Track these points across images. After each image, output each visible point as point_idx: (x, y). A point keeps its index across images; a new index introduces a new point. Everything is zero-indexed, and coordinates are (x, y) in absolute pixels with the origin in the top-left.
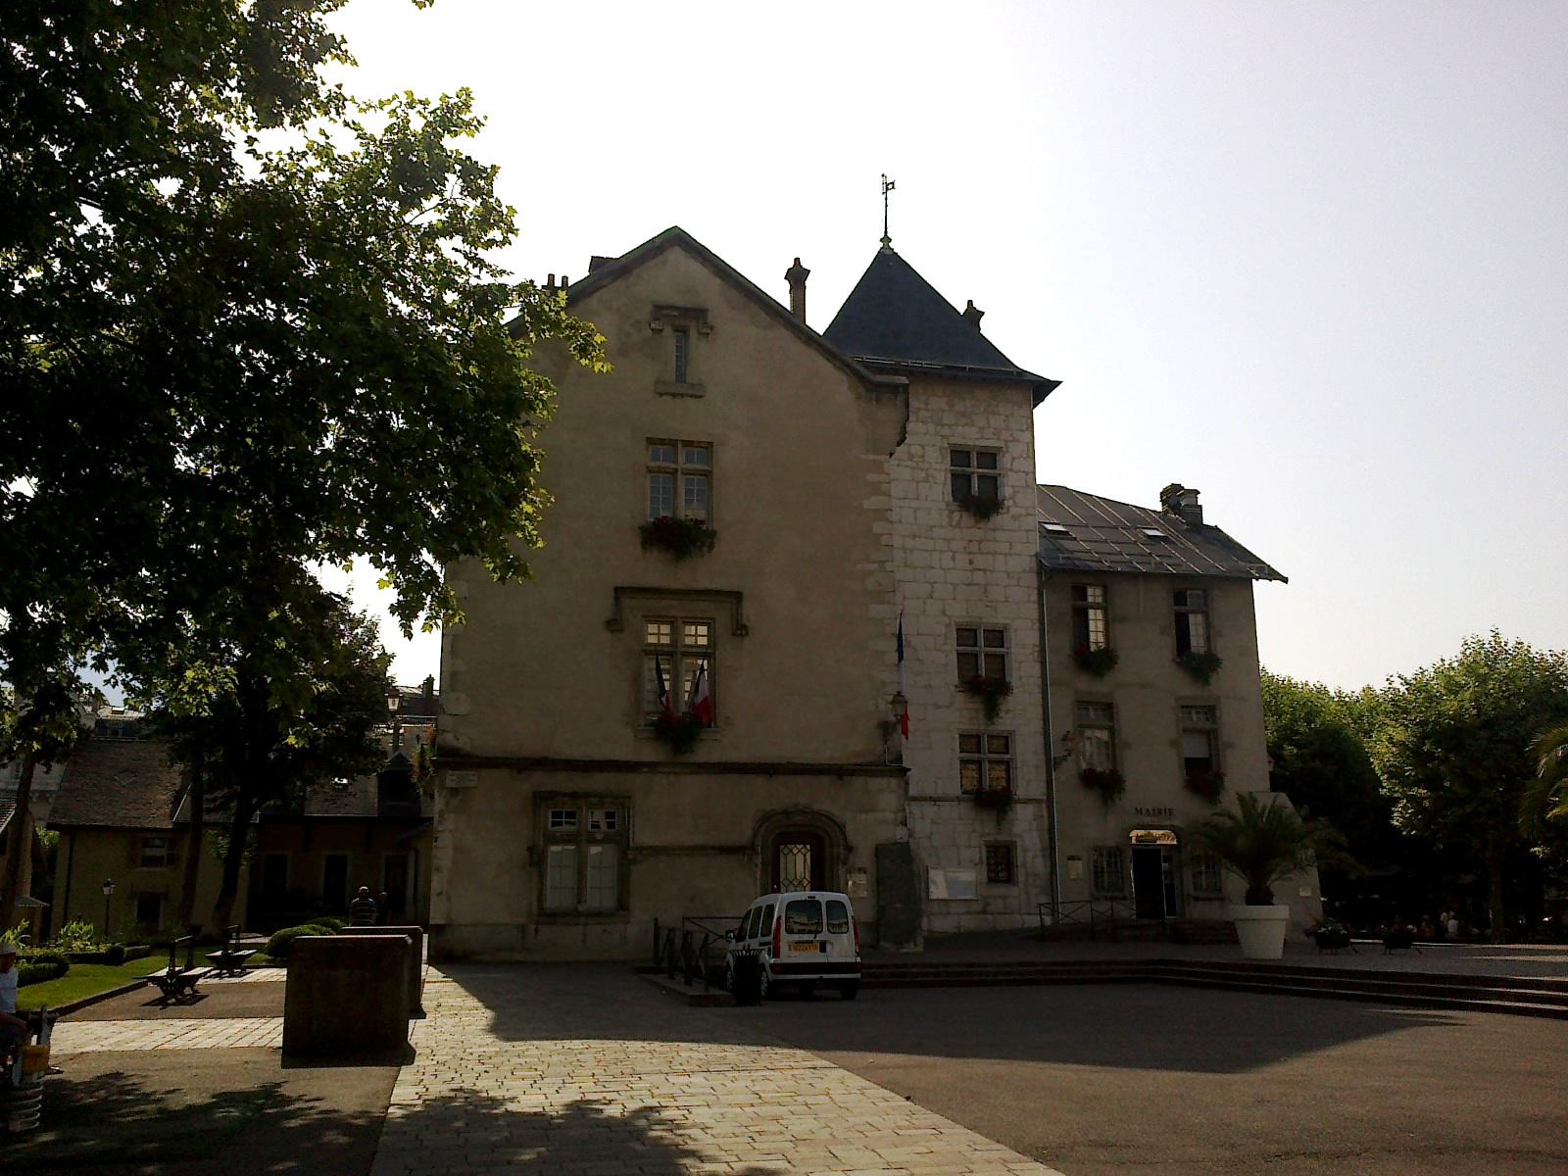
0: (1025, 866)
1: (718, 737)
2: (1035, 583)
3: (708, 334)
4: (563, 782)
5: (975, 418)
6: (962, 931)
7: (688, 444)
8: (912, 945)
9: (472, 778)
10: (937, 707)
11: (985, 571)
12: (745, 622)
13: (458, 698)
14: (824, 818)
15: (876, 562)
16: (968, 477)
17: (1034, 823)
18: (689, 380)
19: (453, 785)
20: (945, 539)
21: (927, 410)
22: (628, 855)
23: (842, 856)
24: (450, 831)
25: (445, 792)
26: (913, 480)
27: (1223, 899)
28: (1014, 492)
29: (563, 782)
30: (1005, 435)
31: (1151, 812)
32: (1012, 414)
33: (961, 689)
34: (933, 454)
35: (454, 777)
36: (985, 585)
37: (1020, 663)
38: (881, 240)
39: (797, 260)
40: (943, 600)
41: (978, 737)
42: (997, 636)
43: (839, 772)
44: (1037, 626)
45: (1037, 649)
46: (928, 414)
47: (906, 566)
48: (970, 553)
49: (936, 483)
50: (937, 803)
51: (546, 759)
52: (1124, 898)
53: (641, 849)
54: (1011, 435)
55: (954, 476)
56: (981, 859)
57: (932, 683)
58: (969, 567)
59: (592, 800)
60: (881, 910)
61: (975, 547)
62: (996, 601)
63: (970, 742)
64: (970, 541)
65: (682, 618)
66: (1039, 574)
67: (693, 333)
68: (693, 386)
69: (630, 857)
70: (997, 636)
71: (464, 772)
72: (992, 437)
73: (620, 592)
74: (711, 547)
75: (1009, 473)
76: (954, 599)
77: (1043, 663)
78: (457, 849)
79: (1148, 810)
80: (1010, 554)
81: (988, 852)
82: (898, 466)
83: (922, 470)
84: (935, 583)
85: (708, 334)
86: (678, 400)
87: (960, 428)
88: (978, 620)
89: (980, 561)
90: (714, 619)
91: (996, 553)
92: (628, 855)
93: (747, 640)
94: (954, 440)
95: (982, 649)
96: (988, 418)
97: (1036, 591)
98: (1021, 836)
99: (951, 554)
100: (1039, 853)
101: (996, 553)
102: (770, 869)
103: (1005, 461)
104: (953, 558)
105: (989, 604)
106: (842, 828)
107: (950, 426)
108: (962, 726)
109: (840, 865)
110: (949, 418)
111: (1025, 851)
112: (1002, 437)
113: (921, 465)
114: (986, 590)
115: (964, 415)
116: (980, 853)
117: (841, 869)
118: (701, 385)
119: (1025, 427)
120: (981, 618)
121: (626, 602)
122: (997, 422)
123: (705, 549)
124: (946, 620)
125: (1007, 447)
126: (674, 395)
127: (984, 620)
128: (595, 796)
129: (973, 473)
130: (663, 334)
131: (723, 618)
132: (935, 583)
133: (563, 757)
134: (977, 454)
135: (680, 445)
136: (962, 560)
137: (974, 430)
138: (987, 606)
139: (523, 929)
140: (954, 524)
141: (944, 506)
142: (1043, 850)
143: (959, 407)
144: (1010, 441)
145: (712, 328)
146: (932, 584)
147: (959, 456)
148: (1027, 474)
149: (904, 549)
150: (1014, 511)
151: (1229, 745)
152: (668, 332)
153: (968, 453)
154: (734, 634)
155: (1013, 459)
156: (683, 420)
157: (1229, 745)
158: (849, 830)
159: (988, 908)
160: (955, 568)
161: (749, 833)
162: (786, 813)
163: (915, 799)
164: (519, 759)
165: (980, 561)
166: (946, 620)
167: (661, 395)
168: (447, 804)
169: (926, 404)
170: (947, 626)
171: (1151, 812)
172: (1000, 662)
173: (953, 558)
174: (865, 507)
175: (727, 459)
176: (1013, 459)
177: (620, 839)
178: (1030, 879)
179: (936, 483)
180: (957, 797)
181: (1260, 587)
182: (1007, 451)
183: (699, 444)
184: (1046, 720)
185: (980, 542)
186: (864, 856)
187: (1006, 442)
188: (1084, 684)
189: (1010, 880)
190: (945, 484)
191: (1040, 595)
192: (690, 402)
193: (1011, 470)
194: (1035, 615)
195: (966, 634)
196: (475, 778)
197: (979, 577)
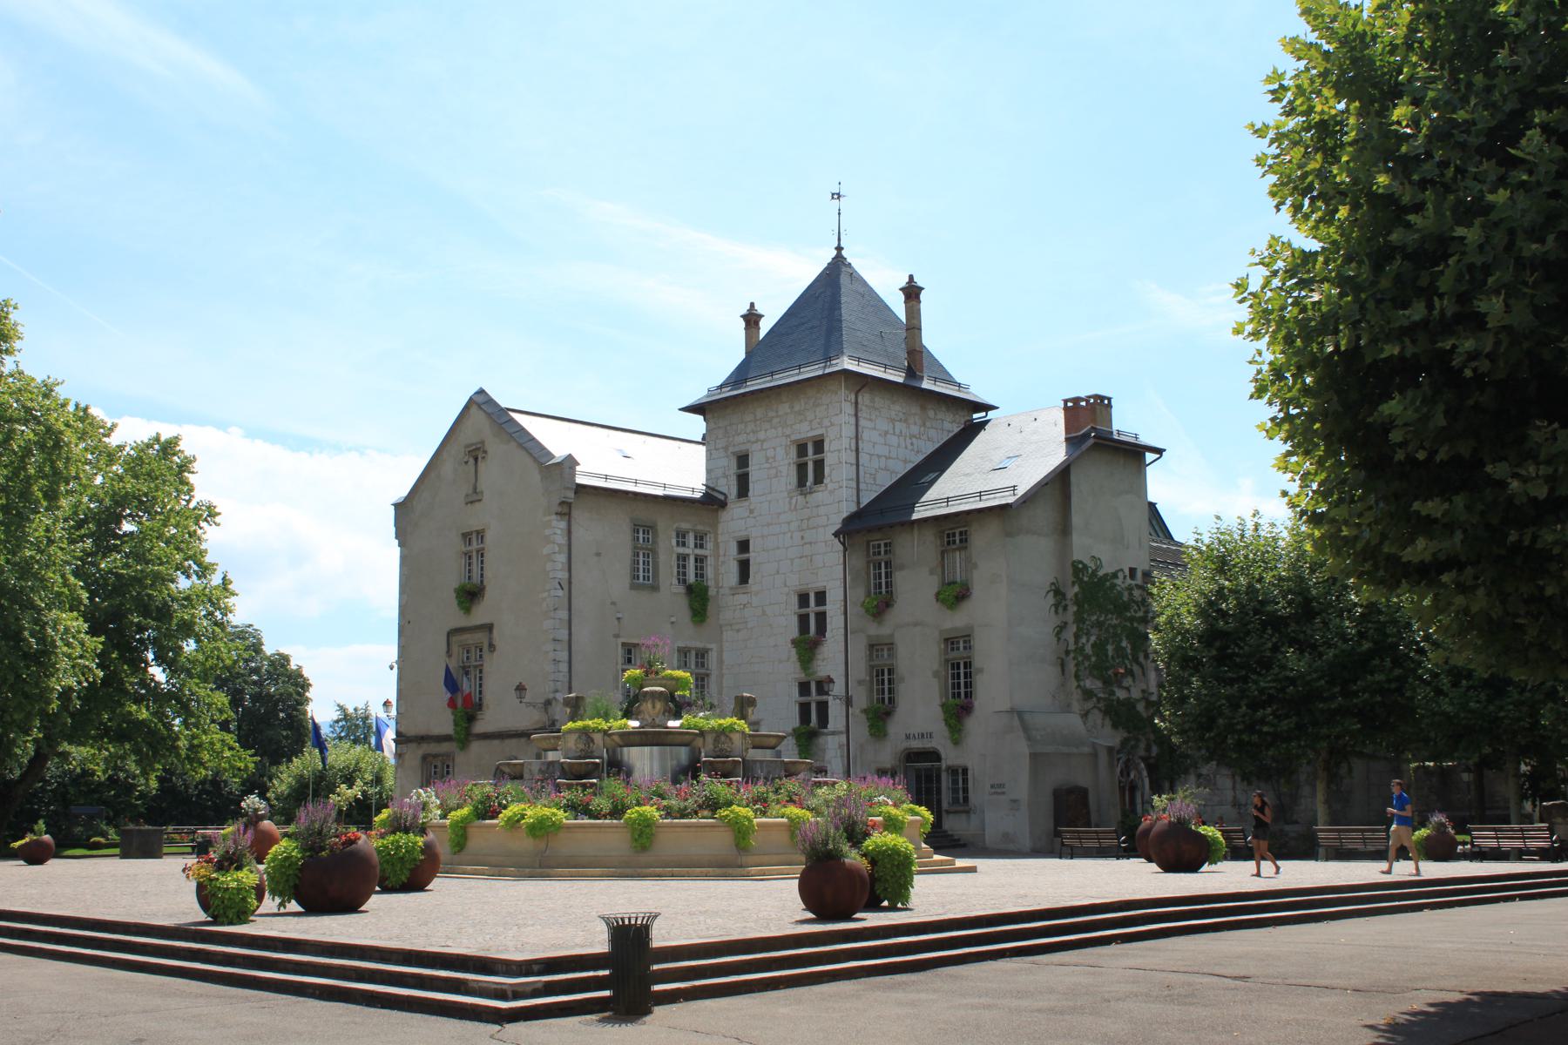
10: (780, 661)
11: (811, 543)
21: (777, 416)
27: (967, 812)
30: (826, 422)
34: (781, 452)
63: (804, 688)
70: (821, 597)
93: (495, 654)
95: (813, 607)
98: (830, 763)
99: (789, 534)
104: (791, 537)
108: (797, 676)
113: (774, 465)
124: (786, 589)
126: (472, 502)
127: (810, 586)
137: (807, 423)
140: (793, 507)
141: (786, 494)
149: (763, 536)
150: (830, 486)
151: (981, 671)
155: (831, 441)
156: (474, 519)
157: (981, 671)
166: (786, 589)
167: (467, 504)
170: (787, 594)
173: (791, 537)
176: (831, 441)
185: (808, 519)
187: (826, 427)
192: (477, 504)
195: (803, 599)
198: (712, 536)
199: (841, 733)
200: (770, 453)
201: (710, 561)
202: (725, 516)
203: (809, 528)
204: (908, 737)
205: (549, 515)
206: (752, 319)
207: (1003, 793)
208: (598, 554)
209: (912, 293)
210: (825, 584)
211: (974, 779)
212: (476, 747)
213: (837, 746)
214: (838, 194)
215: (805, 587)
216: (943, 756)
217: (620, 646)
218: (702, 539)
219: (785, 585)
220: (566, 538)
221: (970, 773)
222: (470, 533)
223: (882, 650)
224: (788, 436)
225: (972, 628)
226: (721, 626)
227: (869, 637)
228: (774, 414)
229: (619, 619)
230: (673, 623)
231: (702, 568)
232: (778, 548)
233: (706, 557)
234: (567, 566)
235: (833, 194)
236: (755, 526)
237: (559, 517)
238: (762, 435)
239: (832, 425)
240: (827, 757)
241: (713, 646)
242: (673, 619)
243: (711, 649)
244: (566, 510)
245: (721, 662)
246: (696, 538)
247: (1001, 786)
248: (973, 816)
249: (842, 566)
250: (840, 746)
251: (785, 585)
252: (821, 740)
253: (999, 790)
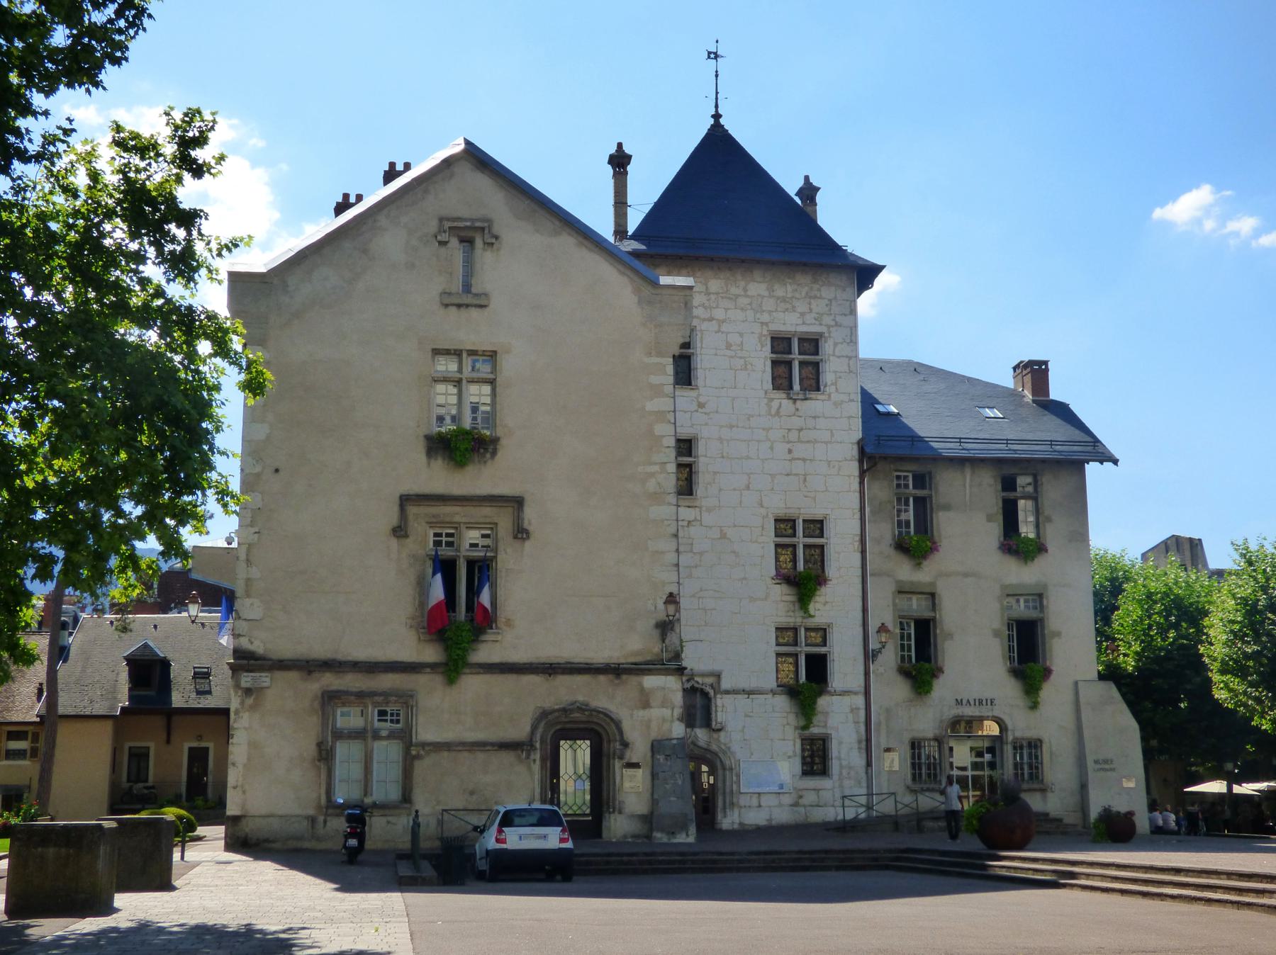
0: (839, 759)
1: (499, 638)
2: (856, 473)
3: (493, 244)
4: (352, 682)
5: (797, 304)
6: (774, 823)
7: (472, 353)
8: (684, 835)
9: (264, 679)
11: (804, 460)
12: (526, 525)
13: (252, 604)
14: (601, 716)
15: (656, 464)
16: (789, 364)
17: (850, 716)
18: (474, 290)
19: (248, 685)
20: (764, 429)
21: (747, 296)
22: (412, 752)
23: (618, 752)
24: (245, 729)
25: (240, 693)
26: (731, 369)
27: (1043, 791)
28: (836, 378)
29: (352, 682)
30: (827, 320)
31: (972, 703)
32: (835, 298)
33: (778, 581)
35: (249, 679)
36: (805, 475)
37: (839, 553)
38: (713, 116)
39: (620, 145)
40: (761, 491)
41: (795, 630)
42: (817, 526)
43: (615, 671)
44: (858, 516)
45: (858, 538)
46: (747, 301)
47: (723, 457)
48: (789, 442)
49: (754, 371)
50: (751, 696)
51: (334, 660)
53: (423, 745)
54: (834, 320)
55: (775, 363)
56: (794, 752)
57: (747, 576)
58: (789, 457)
59: (376, 698)
60: (654, 802)
61: (793, 436)
62: (815, 491)
63: (787, 634)
64: (789, 430)
65: (465, 523)
66: (861, 462)
67: (479, 243)
68: (476, 295)
69: (414, 753)
70: (817, 526)
71: (258, 674)
72: (814, 321)
73: (406, 500)
74: (494, 453)
75: (831, 358)
76: (772, 489)
77: (863, 552)
78: (253, 745)
79: (968, 701)
80: (830, 442)
81: (802, 745)
82: (716, 355)
83: (741, 358)
84: (752, 473)
85: (493, 244)
86: (464, 312)
87: (781, 314)
88: (797, 512)
89: (800, 450)
90: (496, 524)
91: (815, 441)
92: (412, 752)
93: (528, 544)
94: (773, 327)
95: (801, 540)
96: (810, 304)
97: (857, 480)
99: (768, 444)
100: (856, 746)
101: (815, 441)
102: (548, 764)
103: (827, 348)
104: (772, 448)
105: (809, 494)
106: (618, 724)
107: (770, 312)
109: (617, 760)
110: (769, 304)
111: (840, 743)
112: (824, 323)
114: (805, 480)
115: (784, 300)
116: (794, 745)
117: (618, 764)
118: (486, 295)
119: (848, 313)
120: (799, 508)
121: (412, 510)
122: (819, 306)
123: (488, 455)
124: (763, 511)
125: (830, 332)
126: (459, 306)
127: (802, 511)
128: (380, 694)
129: (794, 359)
130: (449, 245)
131: (505, 522)
132: (752, 473)
133: (350, 658)
134: (799, 339)
135: (465, 355)
136: (781, 448)
138: (806, 497)
139: (312, 820)
140: (773, 412)
141: (762, 394)
142: (860, 742)
143: (780, 292)
144: (832, 326)
145: (497, 238)
146: (749, 475)
147: (780, 343)
148: (850, 358)
149: (720, 440)
150: (835, 397)
152: (454, 242)
153: (788, 340)
154: (515, 537)
155: (836, 344)
158: (626, 726)
159: (801, 801)
160: (772, 459)
161: (528, 729)
162: (564, 710)
163: (727, 692)
164: (308, 662)
165: (800, 450)
166: (763, 511)
167: (447, 306)
168: (242, 703)
169: (745, 290)
171: (972, 703)
172: (818, 555)
174: (647, 409)
175: (508, 366)
176: (836, 344)
177: (404, 736)
178: (845, 772)
179: (754, 371)
180: (772, 691)
181: (1092, 469)
182: (830, 337)
183: (484, 353)
184: (865, 610)
185: (800, 430)
186: (639, 750)
187: (829, 327)
188: (905, 571)
189: (824, 772)
190: (764, 372)
191: (861, 483)
192: (474, 313)
193: (834, 355)
194: (857, 505)
195: (785, 525)
196: (268, 679)
197: (798, 467)
199: (856, 693)
200: (734, 339)
203: (800, 441)
205: (660, 354)
206: (620, 161)
207: (1113, 770)
209: (809, 192)
210: (828, 512)
211: (1052, 754)
212: (472, 684)
213: (848, 710)
214: (715, 53)
215: (791, 511)
216: (1010, 727)
219: (762, 507)
222: (461, 351)
223: (911, 599)
224: (767, 324)
225: (1045, 586)
227: (898, 582)
228: (739, 291)
232: (748, 458)
235: (709, 53)
236: (706, 424)
238: (719, 314)
239: (837, 325)
240: (830, 723)
247: (1106, 761)
248: (1049, 795)
249: (857, 495)
250: (854, 710)
251: (762, 507)
252: (823, 702)
253: (1107, 766)
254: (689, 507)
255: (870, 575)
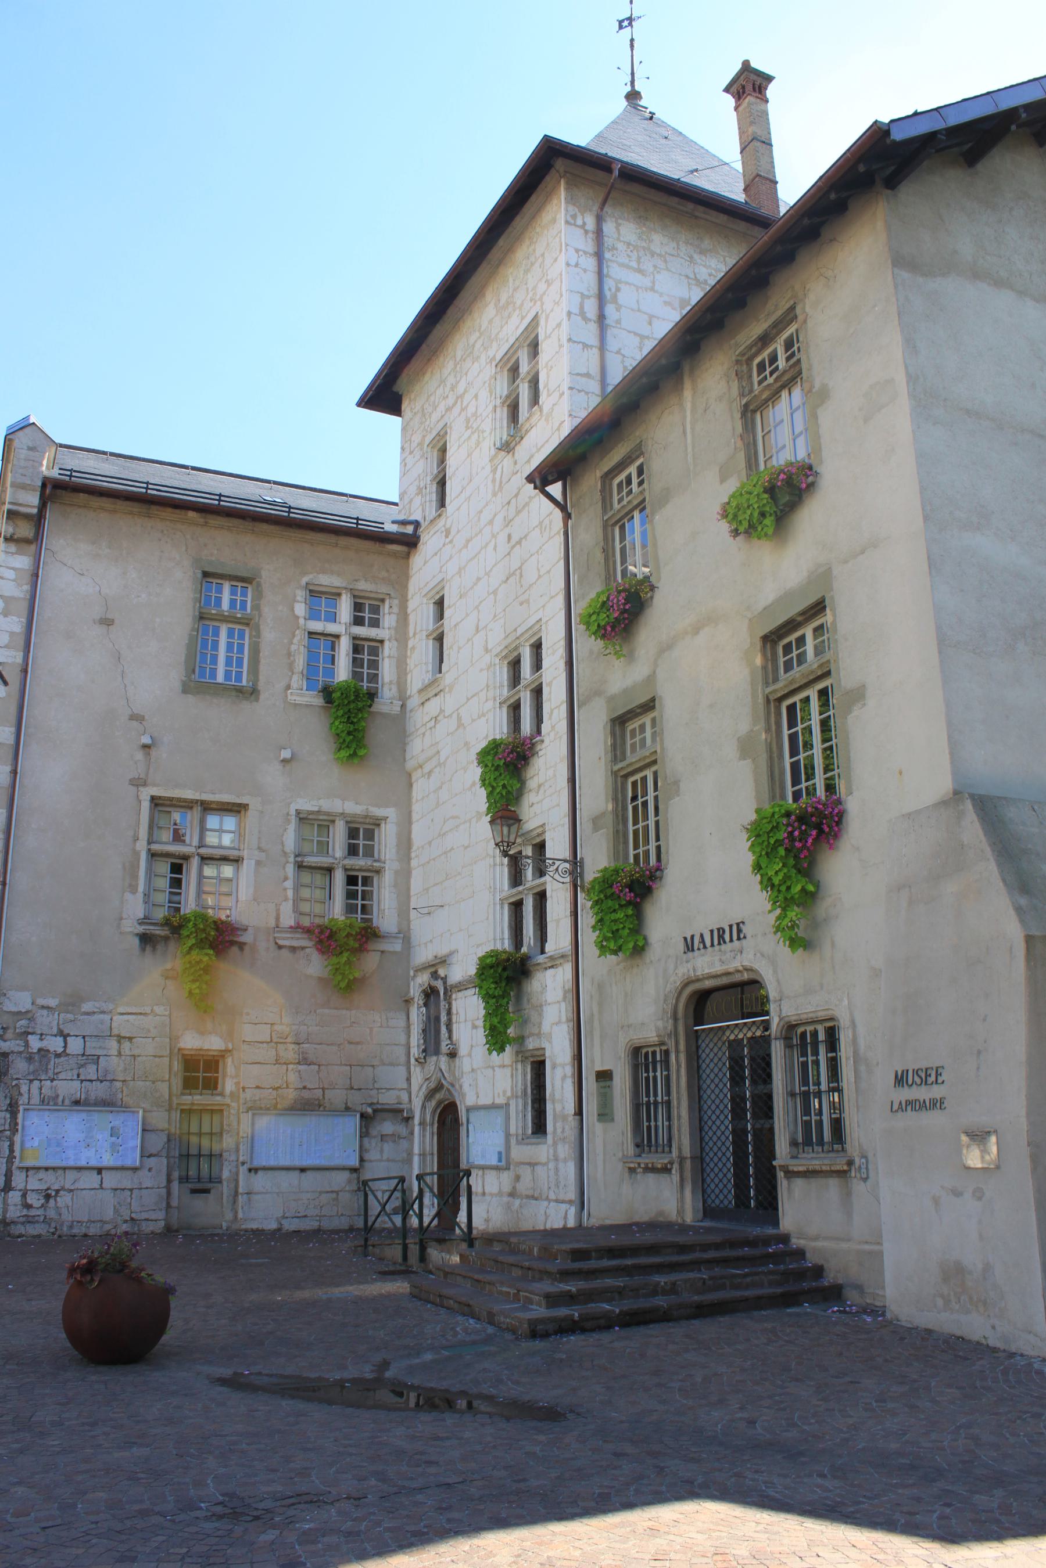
52: (666, 1170)
138: (521, 604)
151: (858, 695)
198: (396, 602)
201: (388, 650)
202: (417, 560)
204: (689, 946)
207: (937, 1104)
208: (107, 622)
211: (857, 1058)
214: (630, 19)
217: (146, 805)
218: (375, 609)
220: (26, 587)
221: (844, 1039)
226: (410, 775)
227: (611, 699)
229: (146, 747)
230: (285, 761)
231: (374, 664)
232: (479, 579)
233: (382, 642)
234: (21, 642)
235: (621, 22)
237: (13, 548)
241: (390, 813)
242: (286, 754)
243: (385, 819)
244: (25, 530)
245: (405, 844)
246: (358, 607)
247: (929, 1076)
253: (922, 1093)
254: (436, 695)
255: (579, 707)
